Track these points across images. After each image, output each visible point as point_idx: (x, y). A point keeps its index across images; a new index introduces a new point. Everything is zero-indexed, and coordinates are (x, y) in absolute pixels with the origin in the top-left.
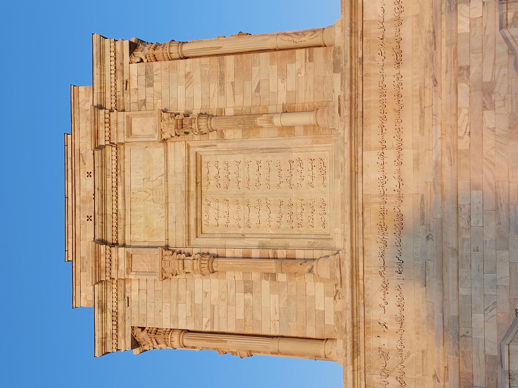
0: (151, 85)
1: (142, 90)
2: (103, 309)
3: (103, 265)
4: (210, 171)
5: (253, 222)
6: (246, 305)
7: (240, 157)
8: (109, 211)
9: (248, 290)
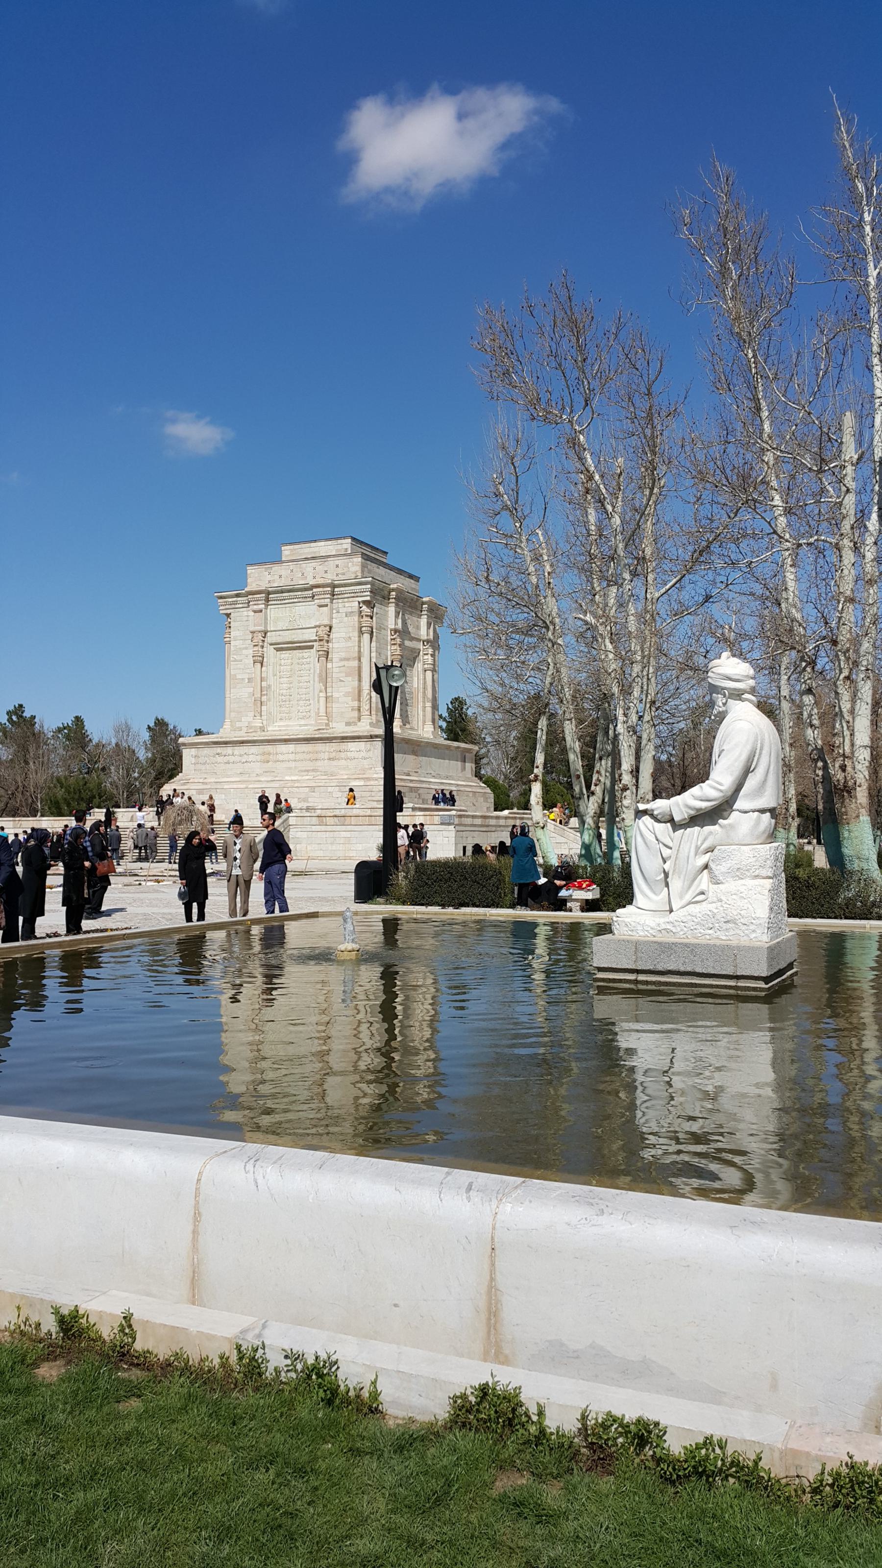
1: (345, 610)
2: (237, 596)
4: (306, 653)
5: (282, 680)
7: (312, 671)
8: (284, 595)
9: (250, 680)
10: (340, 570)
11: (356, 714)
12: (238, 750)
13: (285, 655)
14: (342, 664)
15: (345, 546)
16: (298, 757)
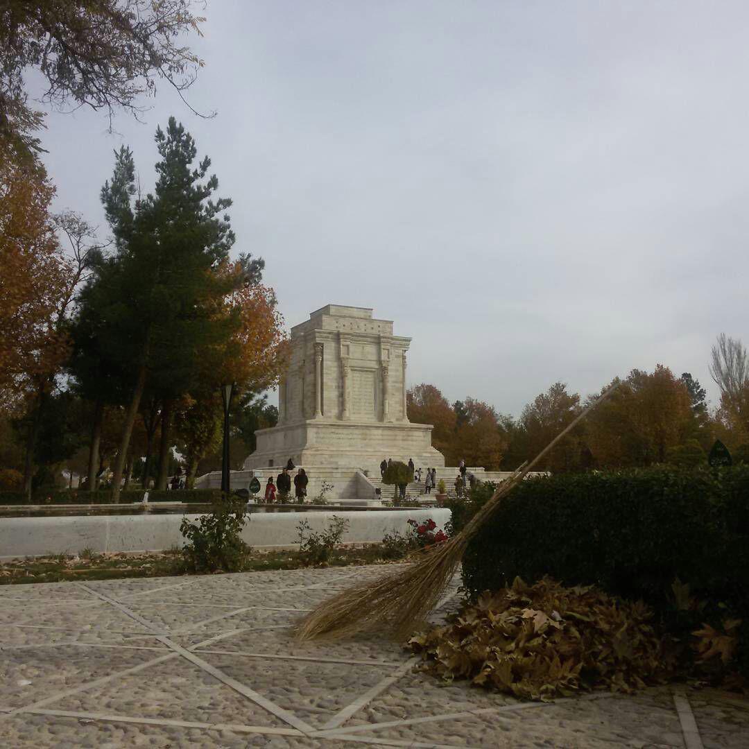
0: (396, 357)
3: (346, 336)
6: (332, 386)
10: (380, 329)
11: (401, 414)
12: (345, 431)
13: (357, 374)
14: (393, 384)
15: (369, 314)
16: (385, 437)
